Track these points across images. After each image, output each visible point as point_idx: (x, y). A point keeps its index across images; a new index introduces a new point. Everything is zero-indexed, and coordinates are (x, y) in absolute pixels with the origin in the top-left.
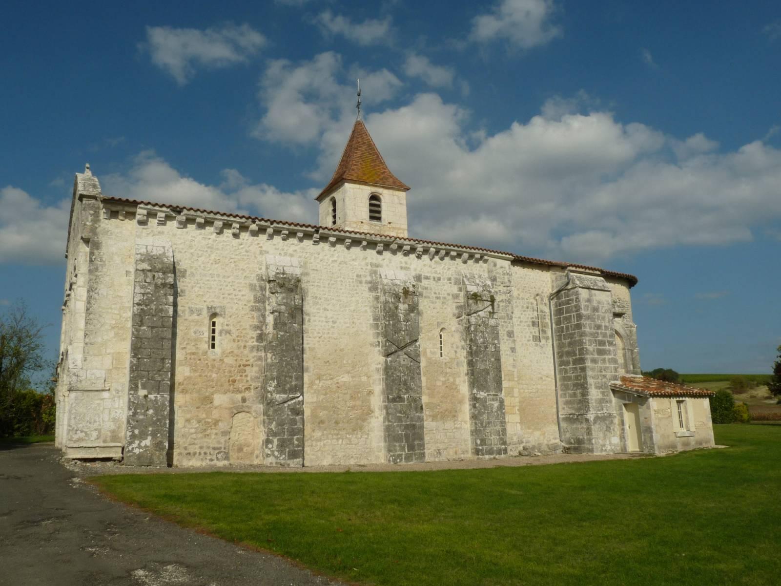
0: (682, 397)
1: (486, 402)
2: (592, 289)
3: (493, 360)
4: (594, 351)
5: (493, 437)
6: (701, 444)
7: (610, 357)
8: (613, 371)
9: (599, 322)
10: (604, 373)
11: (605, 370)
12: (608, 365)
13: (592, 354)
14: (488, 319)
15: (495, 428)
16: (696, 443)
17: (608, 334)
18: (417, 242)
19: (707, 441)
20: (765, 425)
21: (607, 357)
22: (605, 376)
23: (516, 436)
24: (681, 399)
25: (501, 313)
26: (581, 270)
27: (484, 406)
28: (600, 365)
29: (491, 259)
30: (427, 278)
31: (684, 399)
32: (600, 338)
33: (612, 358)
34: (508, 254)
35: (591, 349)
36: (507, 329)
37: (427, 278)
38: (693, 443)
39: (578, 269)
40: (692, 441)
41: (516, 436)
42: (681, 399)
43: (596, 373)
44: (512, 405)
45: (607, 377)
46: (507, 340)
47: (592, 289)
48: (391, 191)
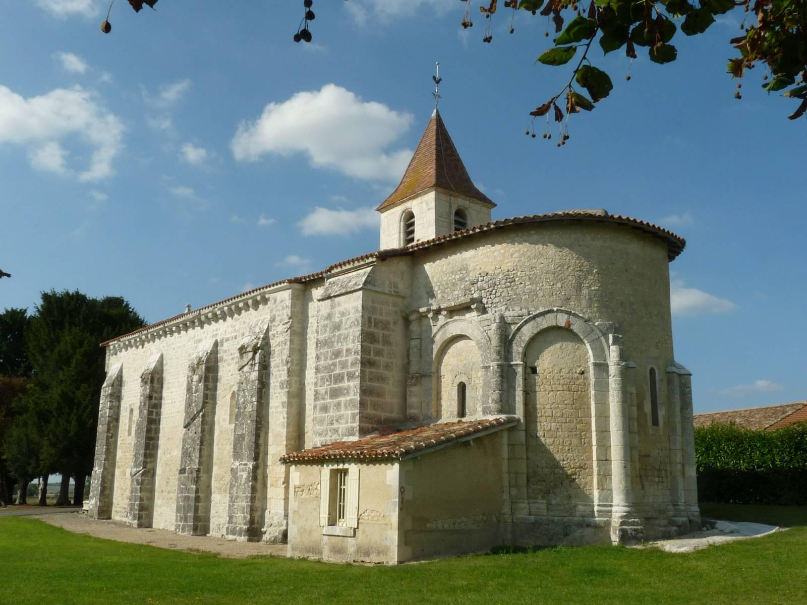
0: (344, 463)
1: (237, 473)
2: (335, 296)
3: (249, 422)
4: (326, 392)
5: (239, 514)
6: (367, 554)
7: (348, 398)
8: (349, 420)
9: (337, 347)
10: (335, 426)
11: (337, 421)
12: (342, 412)
13: (323, 399)
14: (250, 373)
15: (241, 504)
16: (359, 550)
17: (350, 362)
18: (213, 307)
19: (383, 551)
20: (69, 512)
21: (342, 399)
22: (336, 431)
23: (277, 516)
24: (341, 466)
25: (276, 360)
26: (348, 267)
27: (235, 477)
28: (332, 413)
29: (272, 296)
30: (227, 340)
31: (346, 466)
32: (337, 371)
33: (350, 400)
34: (344, 264)
35: (323, 391)
36: (280, 380)
37: (227, 340)
38: (351, 550)
39: (344, 268)
40: (351, 545)
41: (277, 516)
42: (341, 466)
43: (324, 427)
44: (277, 476)
45: (340, 432)
46: (279, 393)
47: (335, 296)
48: (419, 199)
